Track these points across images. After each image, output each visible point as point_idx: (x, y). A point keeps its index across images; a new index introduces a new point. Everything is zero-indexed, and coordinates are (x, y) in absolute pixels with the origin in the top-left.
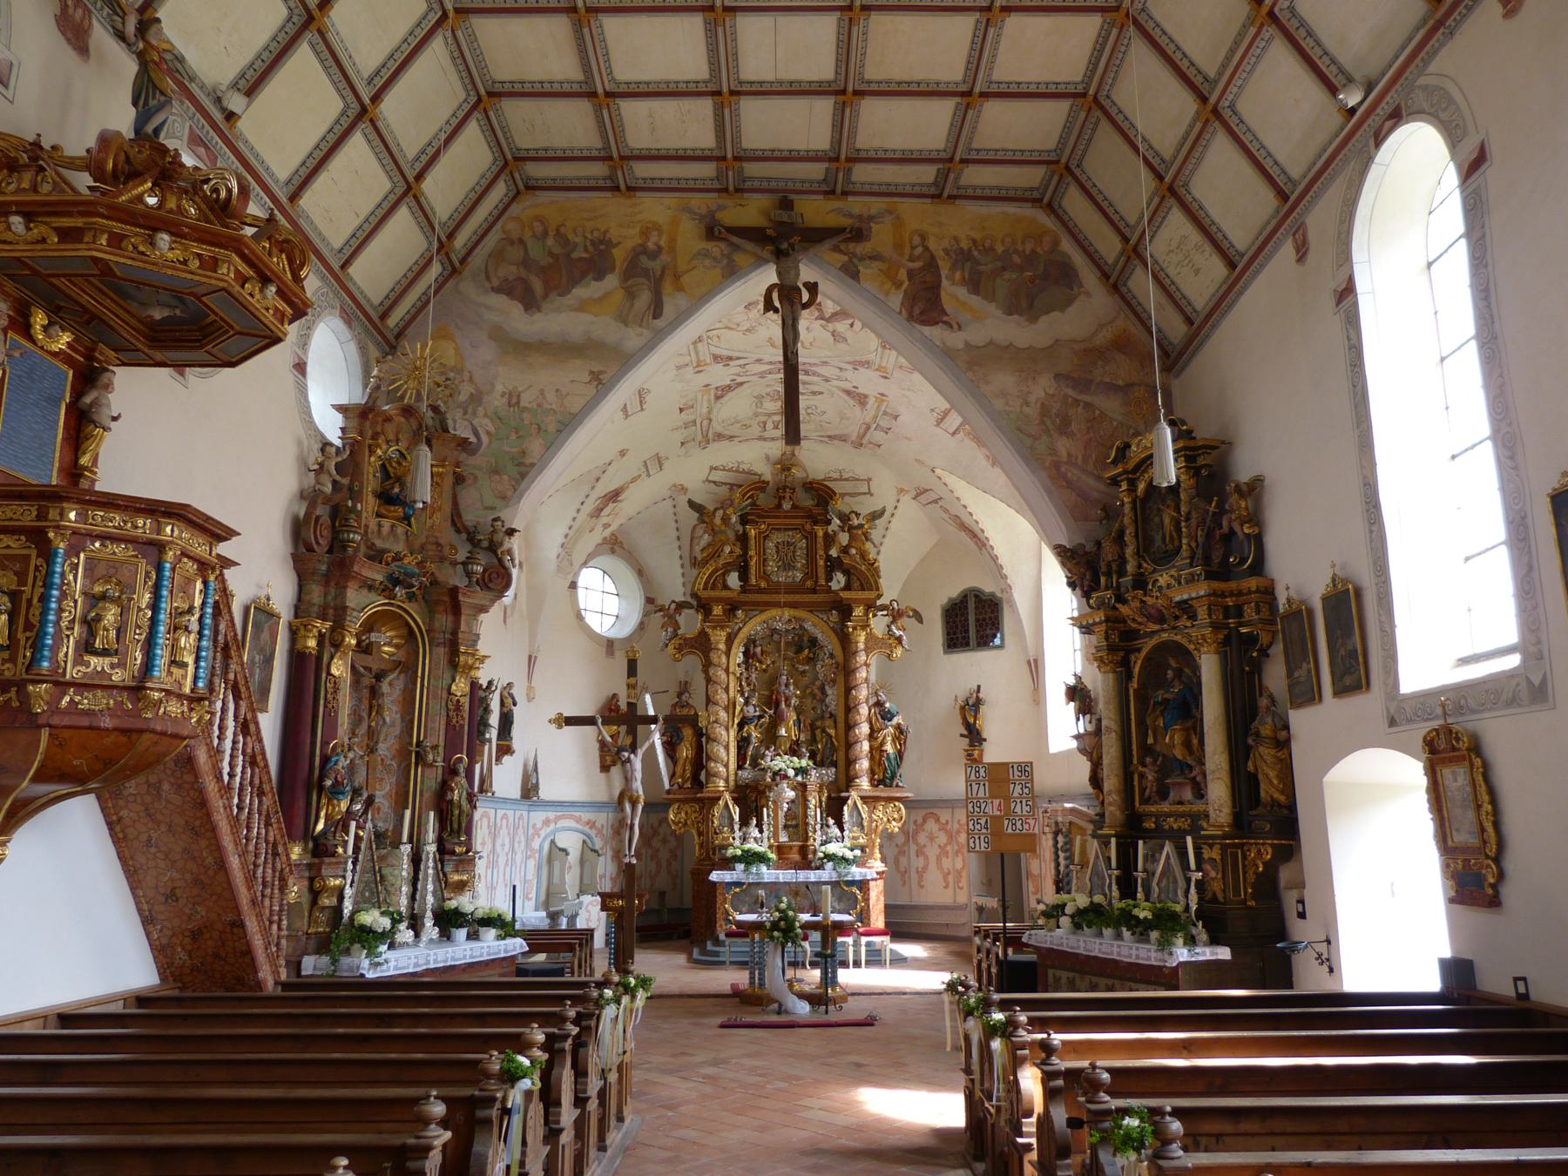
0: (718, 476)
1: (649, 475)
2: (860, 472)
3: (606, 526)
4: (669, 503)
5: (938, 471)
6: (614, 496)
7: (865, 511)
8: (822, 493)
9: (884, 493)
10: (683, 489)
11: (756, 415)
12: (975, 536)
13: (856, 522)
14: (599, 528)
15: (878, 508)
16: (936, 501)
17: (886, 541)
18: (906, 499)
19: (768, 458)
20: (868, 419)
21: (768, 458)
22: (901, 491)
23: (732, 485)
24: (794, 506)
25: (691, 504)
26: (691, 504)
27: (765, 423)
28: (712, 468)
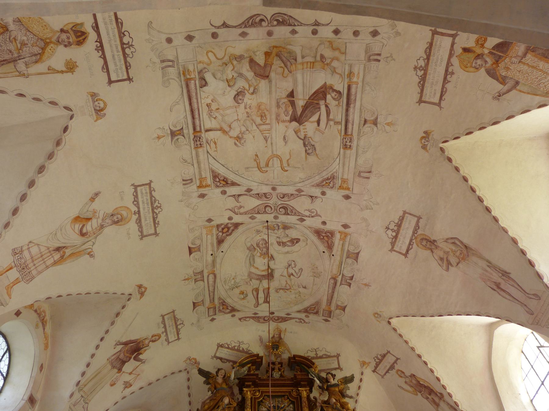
0: (224, 353)
1: (167, 340)
2: (331, 350)
3: (128, 385)
4: (184, 375)
5: (394, 321)
6: (134, 349)
7: (340, 375)
8: (301, 365)
9: (350, 365)
10: (196, 363)
11: (251, 276)
12: (431, 391)
13: (333, 382)
14: (120, 386)
15: (348, 375)
16: (392, 367)
17: (361, 392)
18: (368, 371)
19: (261, 339)
20: (335, 271)
21: (261, 339)
22: (363, 364)
23: (235, 362)
24: (281, 376)
25: (201, 372)
26: (201, 372)
27: (257, 290)
28: (220, 346)
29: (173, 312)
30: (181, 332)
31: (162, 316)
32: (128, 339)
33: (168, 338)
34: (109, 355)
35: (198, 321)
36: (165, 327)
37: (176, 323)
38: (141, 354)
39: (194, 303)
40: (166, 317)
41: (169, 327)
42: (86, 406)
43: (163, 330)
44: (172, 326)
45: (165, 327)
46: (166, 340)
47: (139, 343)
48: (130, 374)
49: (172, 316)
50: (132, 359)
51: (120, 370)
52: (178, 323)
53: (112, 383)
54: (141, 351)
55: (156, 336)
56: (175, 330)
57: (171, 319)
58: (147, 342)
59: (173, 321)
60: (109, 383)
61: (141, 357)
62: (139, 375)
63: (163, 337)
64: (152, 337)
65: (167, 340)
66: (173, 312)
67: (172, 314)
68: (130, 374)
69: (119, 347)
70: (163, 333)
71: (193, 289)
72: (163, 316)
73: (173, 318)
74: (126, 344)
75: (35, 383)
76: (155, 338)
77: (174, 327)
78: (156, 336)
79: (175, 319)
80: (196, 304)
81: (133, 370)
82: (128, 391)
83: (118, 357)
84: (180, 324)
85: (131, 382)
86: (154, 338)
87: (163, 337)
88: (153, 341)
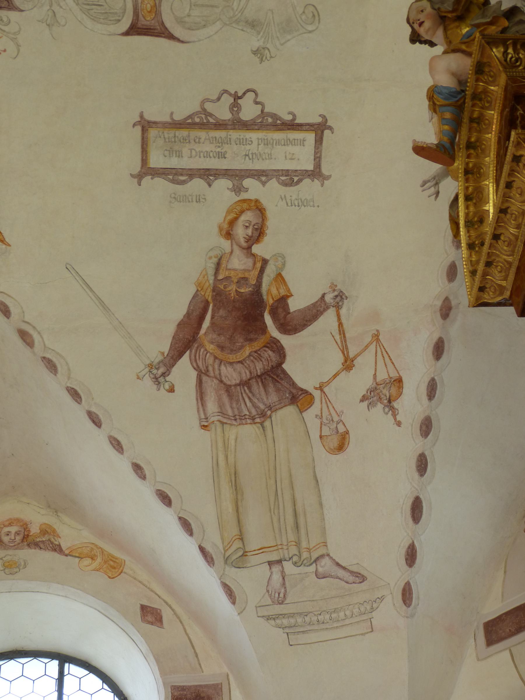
1: (290, 178)
29: (145, 125)
30: (280, 107)
31: (139, 177)
32: (170, 329)
33: (286, 172)
34: (191, 415)
35: (253, 25)
36: (208, 175)
37: (220, 125)
38: (282, 301)
39: (135, 30)
40: (157, 160)
41: (222, 156)
42: (325, 565)
43: (223, 185)
44: (222, 142)
45: (208, 175)
46: (290, 183)
47: (217, 293)
48: (348, 364)
49: (169, 134)
50: (285, 340)
51: (299, 398)
52: (225, 115)
53: (334, 442)
54: (269, 291)
55: (232, 223)
56: (254, 136)
57: (185, 140)
58: (238, 263)
59: (202, 134)
60: (320, 452)
61: (295, 304)
62: (376, 337)
63: (268, 194)
64: (228, 235)
65: (290, 178)
66: (145, 125)
67: (152, 133)
68: (348, 364)
69: (184, 372)
70: (238, 189)
71: (52, 21)
72: (146, 171)
73: (183, 133)
74: (186, 340)
75: (162, 661)
76: (249, 225)
77: (234, 135)
78: (232, 223)
79: (201, 122)
80: (147, 20)
81: (344, 350)
82: (412, 403)
83: (228, 388)
84: (235, 106)
85: (382, 376)
86: (241, 232)
87: (268, 194)
88: (259, 233)
